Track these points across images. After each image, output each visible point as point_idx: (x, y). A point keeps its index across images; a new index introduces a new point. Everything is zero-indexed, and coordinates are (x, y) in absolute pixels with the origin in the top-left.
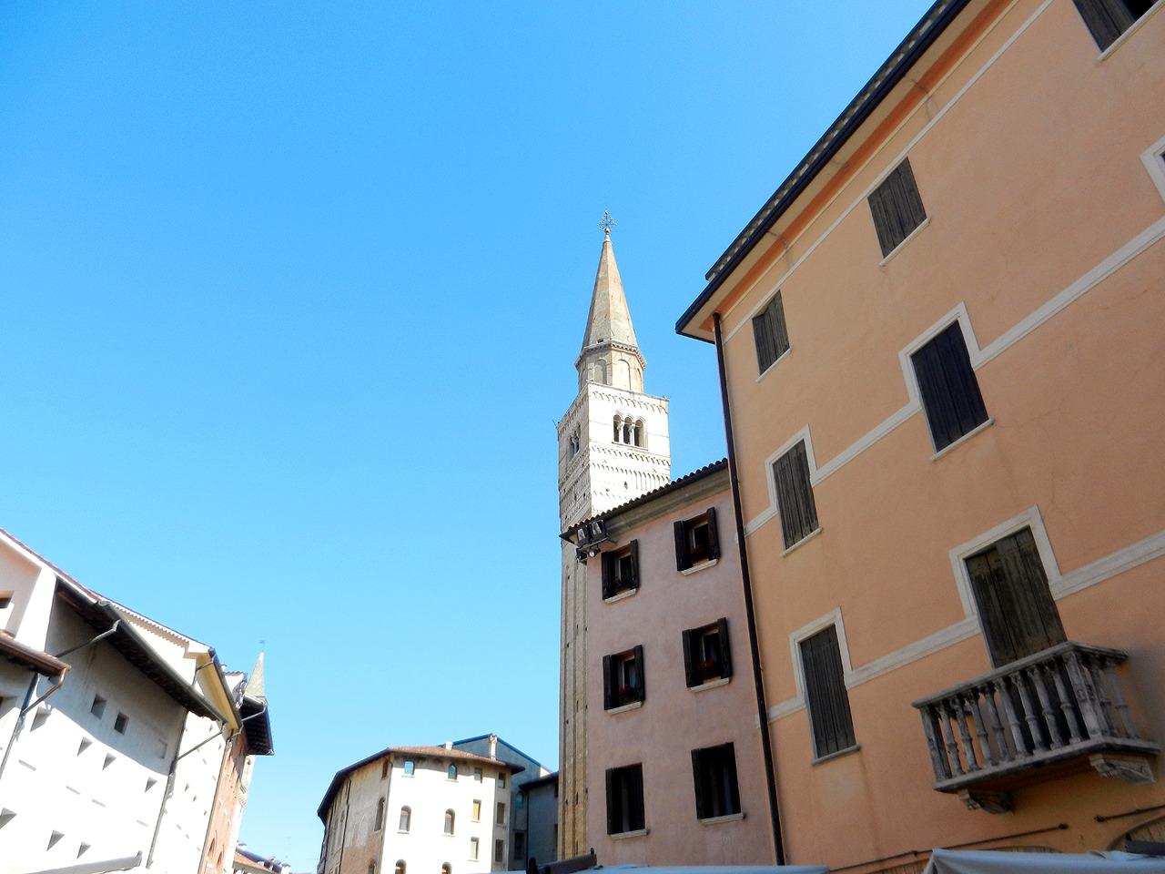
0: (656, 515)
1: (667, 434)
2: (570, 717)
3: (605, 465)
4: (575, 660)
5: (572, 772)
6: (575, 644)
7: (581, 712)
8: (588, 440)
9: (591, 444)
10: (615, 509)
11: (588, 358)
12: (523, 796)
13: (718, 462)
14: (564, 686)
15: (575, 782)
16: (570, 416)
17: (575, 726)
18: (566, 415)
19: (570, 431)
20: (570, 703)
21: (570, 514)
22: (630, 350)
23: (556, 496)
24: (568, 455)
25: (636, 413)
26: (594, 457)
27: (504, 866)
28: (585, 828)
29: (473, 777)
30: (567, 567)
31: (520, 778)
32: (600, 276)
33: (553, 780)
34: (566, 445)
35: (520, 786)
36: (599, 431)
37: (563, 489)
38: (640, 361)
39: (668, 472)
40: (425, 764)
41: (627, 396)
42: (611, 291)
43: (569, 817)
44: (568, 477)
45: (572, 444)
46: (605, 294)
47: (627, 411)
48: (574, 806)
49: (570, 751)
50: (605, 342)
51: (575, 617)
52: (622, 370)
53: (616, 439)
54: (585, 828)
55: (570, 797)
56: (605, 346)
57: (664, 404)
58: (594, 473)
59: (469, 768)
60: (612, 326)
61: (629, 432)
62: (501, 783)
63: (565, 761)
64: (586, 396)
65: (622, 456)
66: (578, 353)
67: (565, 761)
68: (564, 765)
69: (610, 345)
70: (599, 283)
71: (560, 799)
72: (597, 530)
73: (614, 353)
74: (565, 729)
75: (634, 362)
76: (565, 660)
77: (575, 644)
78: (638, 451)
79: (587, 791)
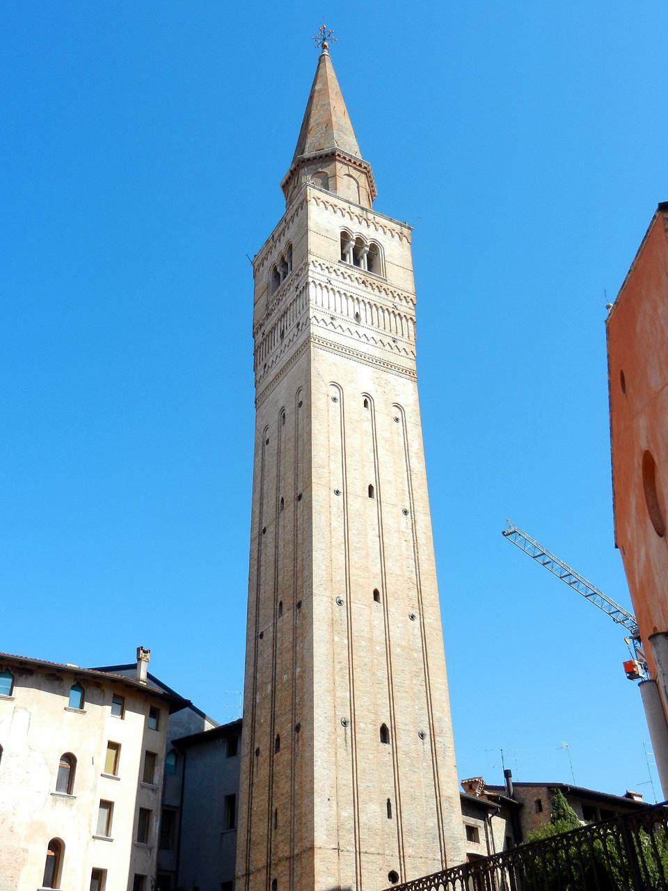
1: (411, 267)
2: (266, 627)
3: (329, 286)
4: (276, 547)
5: (268, 705)
6: (277, 525)
7: (287, 615)
9: (311, 258)
11: (302, 171)
12: (177, 757)
15: (273, 719)
16: (274, 239)
17: (275, 639)
18: (268, 242)
19: (274, 258)
20: (267, 610)
22: (360, 165)
25: (370, 234)
26: (314, 273)
27: (150, 849)
28: (292, 786)
29: (108, 708)
30: (266, 428)
31: (178, 724)
32: (317, 88)
33: (230, 734)
34: (266, 275)
35: (174, 742)
37: (260, 333)
38: (371, 186)
39: (413, 313)
40: (32, 679)
41: (357, 211)
42: (333, 103)
43: (263, 772)
44: (269, 315)
45: (277, 275)
46: (324, 105)
47: (356, 229)
48: (271, 756)
49: (265, 676)
50: (327, 150)
51: (278, 489)
52: (348, 184)
53: (344, 257)
54: (292, 786)
55: (264, 743)
56: (327, 155)
57: (406, 231)
60: (335, 135)
62: (153, 721)
63: (254, 693)
64: (304, 203)
65: (351, 280)
66: (287, 166)
67: (254, 693)
68: (254, 699)
69: (333, 154)
70: (316, 94)
71: (244, 749)
73: (339, 165)
74: (256, 646)
75: (363, 180)
76: (259, 551)
77: (277, 525)
78: (371, 279)
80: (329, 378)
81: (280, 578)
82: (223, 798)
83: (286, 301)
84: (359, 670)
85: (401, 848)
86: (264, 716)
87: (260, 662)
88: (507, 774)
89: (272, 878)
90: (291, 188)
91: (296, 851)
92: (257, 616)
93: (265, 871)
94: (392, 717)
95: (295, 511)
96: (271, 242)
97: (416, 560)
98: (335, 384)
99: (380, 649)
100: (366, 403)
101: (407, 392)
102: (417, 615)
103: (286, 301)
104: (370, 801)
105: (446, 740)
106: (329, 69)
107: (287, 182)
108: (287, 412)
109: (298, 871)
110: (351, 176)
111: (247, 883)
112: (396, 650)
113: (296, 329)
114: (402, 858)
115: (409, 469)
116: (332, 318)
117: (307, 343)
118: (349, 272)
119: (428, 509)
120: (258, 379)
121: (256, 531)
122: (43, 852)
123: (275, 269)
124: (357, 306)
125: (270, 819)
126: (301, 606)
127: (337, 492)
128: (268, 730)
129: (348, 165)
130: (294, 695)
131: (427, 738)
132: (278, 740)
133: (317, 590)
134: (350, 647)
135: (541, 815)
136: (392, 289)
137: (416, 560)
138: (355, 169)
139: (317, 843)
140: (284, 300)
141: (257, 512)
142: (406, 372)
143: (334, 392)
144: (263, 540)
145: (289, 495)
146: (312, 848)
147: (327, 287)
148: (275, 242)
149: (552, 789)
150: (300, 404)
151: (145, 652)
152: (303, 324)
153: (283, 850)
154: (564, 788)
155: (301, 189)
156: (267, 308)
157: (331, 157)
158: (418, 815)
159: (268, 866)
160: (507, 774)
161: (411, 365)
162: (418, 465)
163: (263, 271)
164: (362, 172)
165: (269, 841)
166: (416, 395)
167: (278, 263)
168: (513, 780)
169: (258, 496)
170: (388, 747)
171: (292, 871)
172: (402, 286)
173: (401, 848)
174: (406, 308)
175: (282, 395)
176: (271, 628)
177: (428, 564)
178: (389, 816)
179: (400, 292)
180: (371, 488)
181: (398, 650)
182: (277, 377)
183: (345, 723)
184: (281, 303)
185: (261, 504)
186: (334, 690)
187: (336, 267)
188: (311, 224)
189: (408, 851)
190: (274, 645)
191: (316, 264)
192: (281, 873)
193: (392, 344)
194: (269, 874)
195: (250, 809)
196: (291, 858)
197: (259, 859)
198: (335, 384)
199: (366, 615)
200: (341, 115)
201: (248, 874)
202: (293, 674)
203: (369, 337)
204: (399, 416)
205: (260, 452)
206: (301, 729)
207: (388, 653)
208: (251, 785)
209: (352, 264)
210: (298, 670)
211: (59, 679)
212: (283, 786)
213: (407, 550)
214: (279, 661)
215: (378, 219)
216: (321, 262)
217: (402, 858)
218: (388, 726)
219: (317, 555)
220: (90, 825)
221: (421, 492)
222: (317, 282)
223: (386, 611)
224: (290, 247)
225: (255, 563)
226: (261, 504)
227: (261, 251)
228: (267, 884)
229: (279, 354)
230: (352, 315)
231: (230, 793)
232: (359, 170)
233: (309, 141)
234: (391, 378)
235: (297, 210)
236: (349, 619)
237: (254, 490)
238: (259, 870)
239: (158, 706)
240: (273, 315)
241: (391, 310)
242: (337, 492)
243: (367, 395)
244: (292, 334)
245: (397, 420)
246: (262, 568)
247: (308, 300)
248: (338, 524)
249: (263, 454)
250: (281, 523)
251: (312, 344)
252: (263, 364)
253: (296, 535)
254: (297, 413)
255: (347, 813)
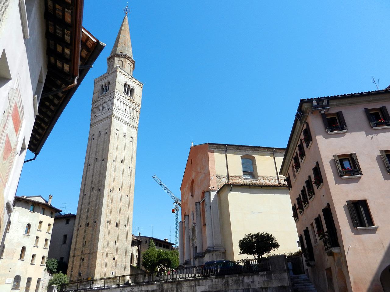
0: (351, 104)
3: (119, 100)
6: (94, 165)
7: (95, 192)
8: (114, 88)
9: (116, 90)
10: (348, 94)
13: (308, 99)
14: (84, 180)
16: (103, 77)
17: (90, 197)
18: (101, 76)
19: (103, 82)
20: (88, 189)
21: (98, 115)
22: (132, 61)
23: (90, 107)
24: (100, 92)
25: (132, 85)
26: (116, 95)
30: (93, 135)
32: (123, 28)
34: (99, 88)
36: (119, 87)
39: (140, 111)
40: (20, 203)
41: (130, 77)
44: (98, 100)
45: (102, 88)
46: (124, 36)
47: (129, 82)
48: (85, 228)
55: (83, 224)
57: (142, 85)
58: (115, 101)
59: (40, 207)
61: (129, 90)
64: (116, 71)
65: (125, 98)
68: (81, 212)
69: (125, 56)
70: (122, 31)
72: (325, 102)
73: (127, 60)
79: (95, 222)
80: (116, 128)
81: (94, 180)
82: (63, 235)
83: (105, 99)
84: (113, 209)
85: (117, 252)
86: (84, 217)
87: (84, 202)
88: (140, 234)
89: (82, 258)
90: (110, 61)
91: (91, 252)
92: (84, 189)
93: (80, 256)
94: (119, 221)
95: (101, 163)
96: (102, 77)
97: (131, 180)
98: (117, 130)
99: (119, 203)
100: (124, 135)
101: (134, 133)
102: (128, 195)
103: (105, 99)
104: (112, 241)
105: (130, 227)
106: (126, 22)
107: (109, 58)
108: (102, 133)
109: (91, 257)
110: (129, 64)
111: (74, 259)
112: (122, 204)
113: (108, 110)
114: (117, 254)
115: (132, 156)
116: (119, 110)
117: (111, 116)
118: (125, 96)
119: (135, 167)
120: (92, 118)
121: (86, 165)
122: (20, 250)
123: (102, 86)
124: (126, 107)
125: (83, 244)
126: (100, 190)
127: (114, 161)
128: (85, 221)
129: (128, 60)
130: (95, 213)
131: (126, 226)
132: (88, 223)
133: (106, 187)
134: (112, 203)
135: (146, 244)
136: (135, 103)
137: (131, 180)
138: (131, 61)
139: (98, 251)
140: (105, 98)
141: (88, 159)
142: (135, 128)
143: (116, 132)
144: (89, 168)
145: (100, 158)
146: (97, 252)
147: (119, 100)
148: (104, 78)
149: (150, 238)
150: (106, 133)
151: (52, 196)
152: (110, 109)
153: (87, 251)
154: (153, 239)
155: (113, 62)
156: (98, 98)
157: (125, 56)
158: (121, 245)
159: (82, 255)
160: (140, 234)
161: (137, 126)
162: (134, 155)
163: (98, 85)
164: (132, 63)
165: (82, 248)
166: (137, 135)
167: (104, 85)
168: (141, 235)
169: (88, 154)
170: (117, 228)
171: (89, 257)
172: (138, 102)
173: (117, 252)
174: (138, 109)
175: (100, 127)
176: (89, 194)
177: (133, 182)
178: (115, 245)
179: (137, 104)
180: (122, 160)
181: (123, 204)
182: (98, 121)
183: (108, 222)
184: (103, 99)
185: (89, 157)
186: (106, 214)
187: (122, 94)
188: (117, 79)
189: (118, 253)
190: (90, 198)
191: (117, 92)
192: (86, 258)
193: (133, 119)
194: (81, 257)
195: (76, 240)
196: (89, 254)
197: (78, 253)
198: (117, 130)
199: (116, 194)
200: (129, 41)
201: (74, 256)
202: (95, 208)
203: (128, 116)
204: (132, 140)
205: (90, 141)
206: (96, 222)
207: (120, 205)
208: (77, 234)
209: (126, 93)
210: (97, 207)
211: (28, 203)
212: (89, 236)
213: (129, 178)
214: (90, 203)
215: (135, 80)
216: (119, 92)
217: (117, 254)
218: (118, 223)
219: (107, 178)
220: (33, 243)
221: (134, 163)
222: (117, 98)
223: (121, 194)
224: (109, 83)
225: (85, 173)
226: (89, 157)
227: (98, 78)
228: (81, 259)
229: (101, 115)
230: (124, 109)
231: (66, 234)
232: (131, 62)
233: (119, 48)
234: (131, 129)
235: (113, 72)
236: (113, 195)
237: (87, 152)
238: (78, 256)
239: (52, 211)
240: (100, 101)
241: (134, 109)
242: (114, 161)
243: (124, 133)
244: (106, 110)
245: (131, 141)
246: (87, 176)
247: (113, 103)
248: (113, 170)
249: (91, 142)
250: (96, 165)
251: (113, 117)
252: (94, 115)
253: (100, 170)
254: (105, 135)
255: (106, 244)
